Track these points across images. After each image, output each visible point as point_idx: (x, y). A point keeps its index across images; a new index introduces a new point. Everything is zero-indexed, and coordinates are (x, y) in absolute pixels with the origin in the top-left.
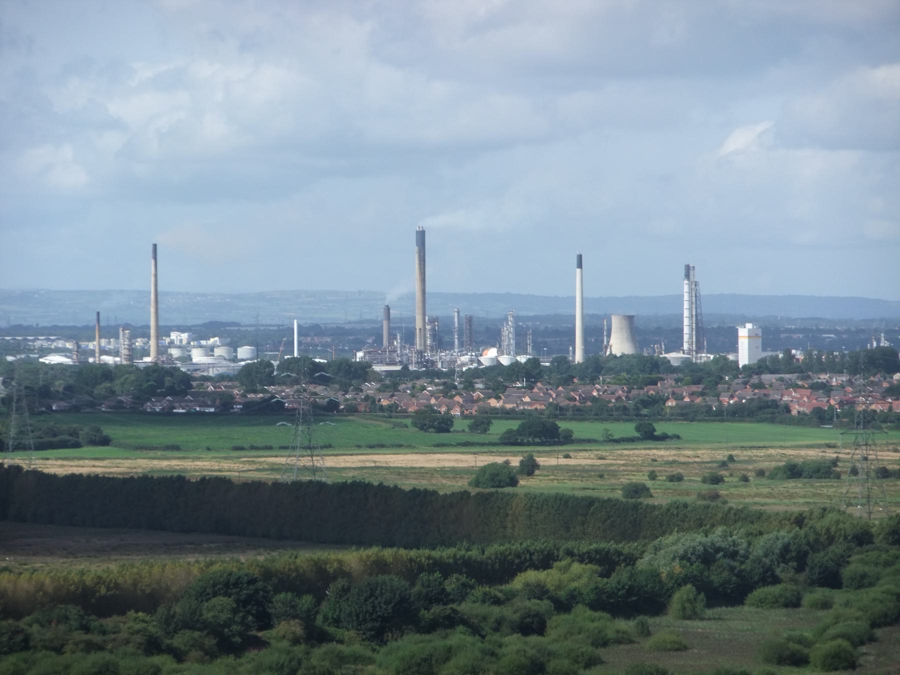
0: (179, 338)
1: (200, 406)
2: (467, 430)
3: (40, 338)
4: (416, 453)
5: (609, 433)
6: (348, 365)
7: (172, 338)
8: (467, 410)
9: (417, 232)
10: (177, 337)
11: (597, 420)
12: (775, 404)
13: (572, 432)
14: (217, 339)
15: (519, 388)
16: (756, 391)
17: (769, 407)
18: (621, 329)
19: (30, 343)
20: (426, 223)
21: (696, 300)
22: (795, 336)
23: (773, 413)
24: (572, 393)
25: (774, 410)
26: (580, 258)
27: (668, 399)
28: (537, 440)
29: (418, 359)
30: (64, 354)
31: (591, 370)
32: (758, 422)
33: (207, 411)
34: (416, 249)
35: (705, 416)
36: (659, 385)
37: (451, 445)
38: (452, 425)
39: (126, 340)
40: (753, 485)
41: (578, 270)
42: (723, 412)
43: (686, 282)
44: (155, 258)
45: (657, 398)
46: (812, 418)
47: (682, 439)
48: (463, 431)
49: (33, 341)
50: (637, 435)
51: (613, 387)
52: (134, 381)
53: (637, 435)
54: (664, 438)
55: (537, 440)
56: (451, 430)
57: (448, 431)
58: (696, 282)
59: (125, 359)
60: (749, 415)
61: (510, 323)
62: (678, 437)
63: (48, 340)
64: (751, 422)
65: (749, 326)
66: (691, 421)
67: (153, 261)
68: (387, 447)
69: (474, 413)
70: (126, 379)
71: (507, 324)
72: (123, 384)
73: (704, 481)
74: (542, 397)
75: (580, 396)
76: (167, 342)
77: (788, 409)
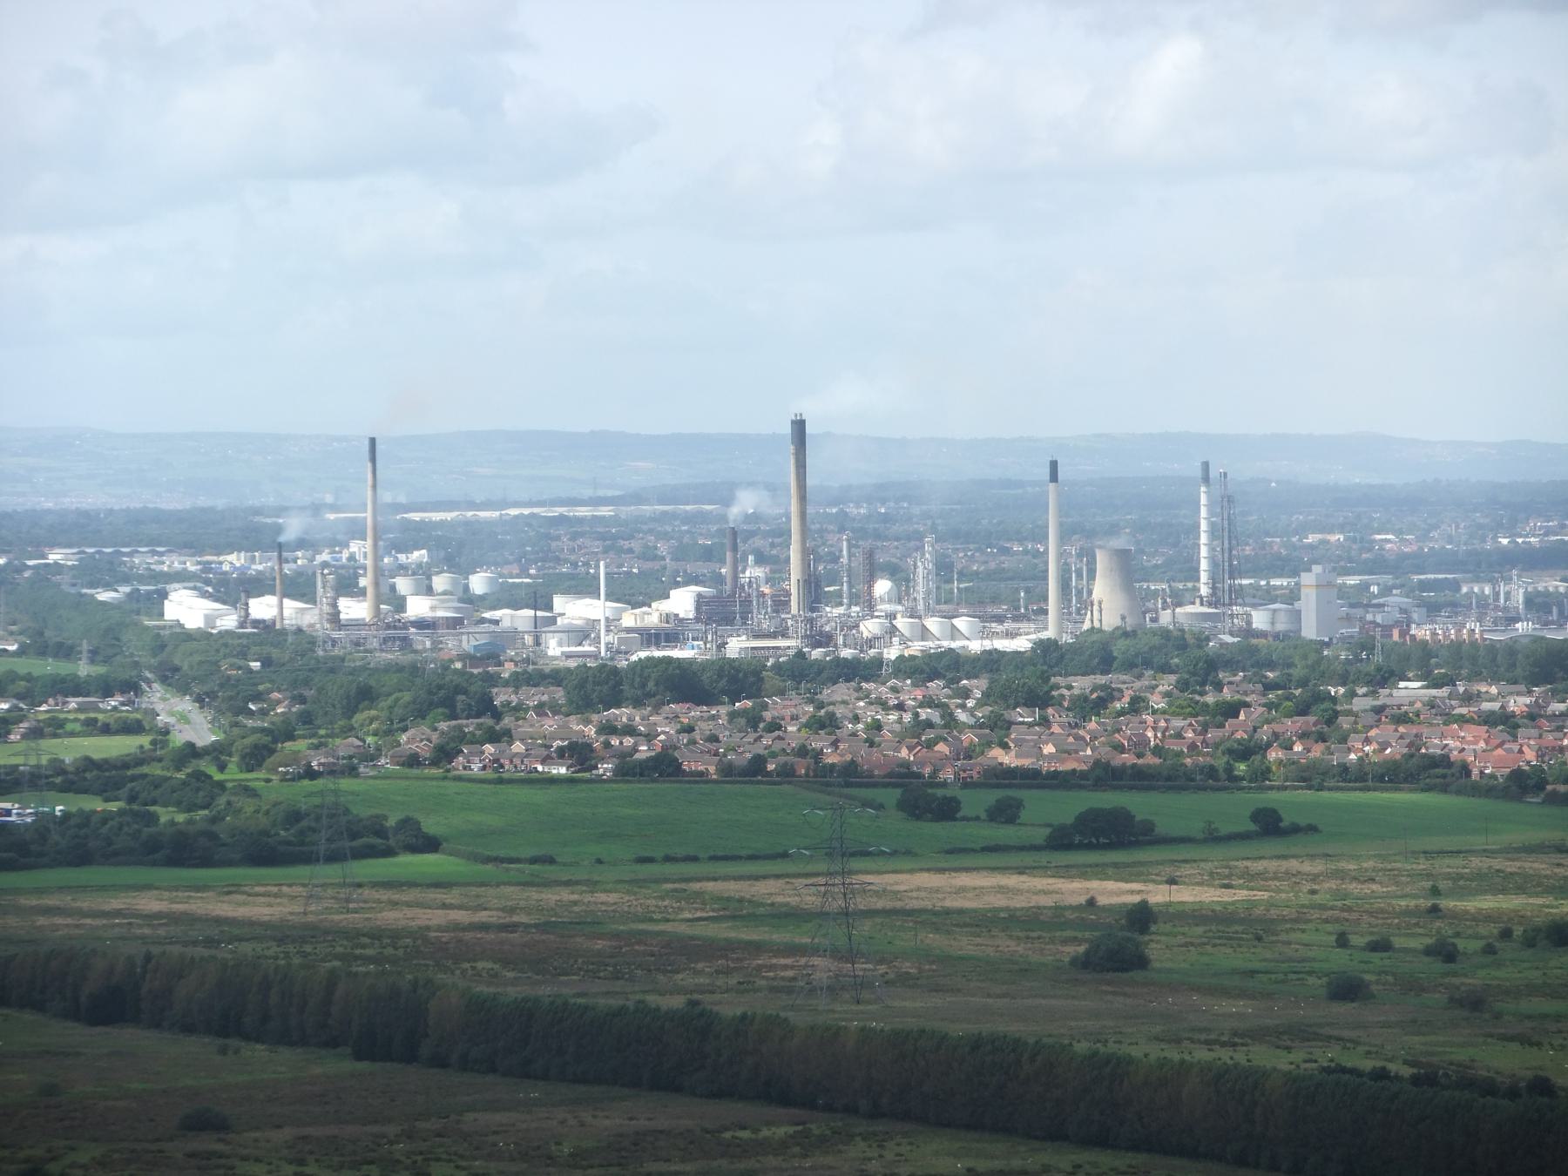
0: (363, 550)
1: (543, 762)
2: (983, 816)
3: (140, 549)
4: (928, 870)
5: (1213, 826)
6: (733, 668)
7: (351, 550)
8: (964, 771)
9: (793, 422)
10: (360, 549)
11: (1170, 788)
12: (1443, 761)
13: (1153, 824)
14: (424, 552)
15: (1030, 725)
16: (1401, 729)
17: (1436, 766)
18: (1111, 571)
19: (125, 559)
20: (810, 409)
21: (1229, 524)
22: (1334, 538)
23: (1444, 776)
24: (1117, 735)
25: (1445, 771)
26: (1054, 466)
27: (1269, 745)
28: (1102, 840)
29: (806, 630)
30: (191, 585)
31: (1096, 660)
32: (1423, 790)
33: (555, 772)
34: (792, 448)
35: (1338, 782)
36: (1242, 717)
37: (974, 851)
38: (958, 809)
39: (329, 590)
40: (1508, 963)
41: (1052, 486)
42: (1366, 774)
43: (1203, 489)
44: (373, 459)
45: (1252, 743)
46: (1509, 786)
47: (1321, 832)
48: (977, 818)
49: (130, 554)
50: (1253, 827)
51: (1178, 723)
52: (409, 703)
53: (1253, 827)
54: (1295, 830)
55: (1102, 840)
56: (958, 815)
57: (955, 819)
58: (1229, 497)
59: (328, 620)
60: (1405, 780)
61: (927, 556)
62: (1312, 829)
63: (154, 553)
64: (1411, 791)
65: (1317, 569)
66: (1318, 790)
67: (369, 465)
68: (875, 855)
69: (976, 776)
70: (397, 700)
71: (923, 555)
72: (391, 708)
73: (1428, 951)
74: (1072, 743)
75: (1130, 739)
76: (344, 560)
77: (1465, 769)
